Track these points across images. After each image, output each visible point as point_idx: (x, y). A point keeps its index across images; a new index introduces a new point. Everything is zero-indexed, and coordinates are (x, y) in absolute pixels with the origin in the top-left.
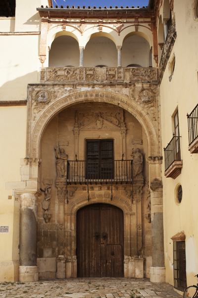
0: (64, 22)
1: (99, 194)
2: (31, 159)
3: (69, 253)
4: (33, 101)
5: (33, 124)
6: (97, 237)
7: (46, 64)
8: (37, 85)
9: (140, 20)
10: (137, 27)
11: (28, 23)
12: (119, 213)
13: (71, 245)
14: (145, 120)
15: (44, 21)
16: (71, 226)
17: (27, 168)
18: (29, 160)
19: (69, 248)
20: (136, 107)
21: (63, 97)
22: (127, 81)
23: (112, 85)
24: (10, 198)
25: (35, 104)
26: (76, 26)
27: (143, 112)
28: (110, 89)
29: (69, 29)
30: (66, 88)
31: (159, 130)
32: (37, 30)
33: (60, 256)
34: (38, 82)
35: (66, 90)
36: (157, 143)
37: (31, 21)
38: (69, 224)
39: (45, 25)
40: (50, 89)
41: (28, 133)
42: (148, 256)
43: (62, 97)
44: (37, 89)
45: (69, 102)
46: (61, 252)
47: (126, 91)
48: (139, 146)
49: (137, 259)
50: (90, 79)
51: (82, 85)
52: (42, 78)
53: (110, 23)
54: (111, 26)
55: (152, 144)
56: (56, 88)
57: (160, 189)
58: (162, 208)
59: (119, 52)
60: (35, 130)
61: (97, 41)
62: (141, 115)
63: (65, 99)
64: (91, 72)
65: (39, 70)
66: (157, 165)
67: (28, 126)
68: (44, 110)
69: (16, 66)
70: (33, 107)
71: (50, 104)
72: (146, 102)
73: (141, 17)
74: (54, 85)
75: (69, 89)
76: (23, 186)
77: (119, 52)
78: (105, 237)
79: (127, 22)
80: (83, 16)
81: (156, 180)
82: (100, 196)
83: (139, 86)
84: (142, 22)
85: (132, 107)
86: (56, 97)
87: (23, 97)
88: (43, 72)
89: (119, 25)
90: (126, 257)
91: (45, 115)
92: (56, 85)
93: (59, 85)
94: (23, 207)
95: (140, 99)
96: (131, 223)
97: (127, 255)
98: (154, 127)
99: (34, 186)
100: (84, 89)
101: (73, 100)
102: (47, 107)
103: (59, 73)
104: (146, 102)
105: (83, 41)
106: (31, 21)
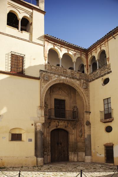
0: (54, 44)
1: (62, 125)
2: (42, 107)
3: (48, 151)
4: (42, 79)
5: (42, 90)
6: (58, 144)
7: (47, 62)
8: (44, 71)
9: (82, 52)
10: (81, 55)
11: (38, 39)
12: (67, 133)
13: (49, 148)
14: (84, 95)
15: (46, 41)
16: (49, 139)
17: (40, 111)
18: (41, 107)
19: (48, 149)
20: (81, 90)
21: (55, 79)
22: (78, 78)
23: (73, 78)
24: (32, 125)
25: (43, 80)
26: (59, 47)
27: (83, 92)
28: (72, 80)
29: (56, 48)
30: (56, 76)
32: (43, 44)
33: (45, 153)
34: (44, 69)
35: (56, 77)
36: (88, 106)
37: (40, 38)
38: (48, 138)
39: (46, 43)
40: (49, 74)
41: (40, 94)
42: (80, 152)
43: (55, 79)
44: (44, 73)
46: (45, 151)
47: (78, 82)
48: (75, 105)
49: (75, 153)
50: (65, 74)
51: (62, 75)
52: (46, 68)
54: (72, 52)
55: (86, 106)
56: (52, 75)
57: (90, 125)
58: (90, 133)
59: (74, 64)
61: (66, 56)
62: (82, 93)
63: (55, 81)
64: (65, 71)
65: (44, 64)
67: (41, 91)
68: (47, 84)
69: (34, 59)
70: (42, 82)
72: (85, 89)
73: (83, 52)
74: (51, 73)
75: (57, 76)
76: (38, 119)
77: (74, 64)
78: (61, 144)
79: (78, 52)
80: (63, 44)
81: (88, 121)
83: (82, 81)
84: (83, 54)
85: (79, 89)
87: (38, 76)
88: (45, 65)
89: (75, 52)
91: (47, 87)
92: (52, 73)
93: (53, 73)
94: (38, 130)
95: (83, 86)
96: (72, 138)
97: (70, 151)
98: (87, 99)
99: (43, 120)
100: (63, 78)
101: (58, 82)
102: (48, 83)
103: (53, 67)
104: (85, 89)
106: (40, 38)
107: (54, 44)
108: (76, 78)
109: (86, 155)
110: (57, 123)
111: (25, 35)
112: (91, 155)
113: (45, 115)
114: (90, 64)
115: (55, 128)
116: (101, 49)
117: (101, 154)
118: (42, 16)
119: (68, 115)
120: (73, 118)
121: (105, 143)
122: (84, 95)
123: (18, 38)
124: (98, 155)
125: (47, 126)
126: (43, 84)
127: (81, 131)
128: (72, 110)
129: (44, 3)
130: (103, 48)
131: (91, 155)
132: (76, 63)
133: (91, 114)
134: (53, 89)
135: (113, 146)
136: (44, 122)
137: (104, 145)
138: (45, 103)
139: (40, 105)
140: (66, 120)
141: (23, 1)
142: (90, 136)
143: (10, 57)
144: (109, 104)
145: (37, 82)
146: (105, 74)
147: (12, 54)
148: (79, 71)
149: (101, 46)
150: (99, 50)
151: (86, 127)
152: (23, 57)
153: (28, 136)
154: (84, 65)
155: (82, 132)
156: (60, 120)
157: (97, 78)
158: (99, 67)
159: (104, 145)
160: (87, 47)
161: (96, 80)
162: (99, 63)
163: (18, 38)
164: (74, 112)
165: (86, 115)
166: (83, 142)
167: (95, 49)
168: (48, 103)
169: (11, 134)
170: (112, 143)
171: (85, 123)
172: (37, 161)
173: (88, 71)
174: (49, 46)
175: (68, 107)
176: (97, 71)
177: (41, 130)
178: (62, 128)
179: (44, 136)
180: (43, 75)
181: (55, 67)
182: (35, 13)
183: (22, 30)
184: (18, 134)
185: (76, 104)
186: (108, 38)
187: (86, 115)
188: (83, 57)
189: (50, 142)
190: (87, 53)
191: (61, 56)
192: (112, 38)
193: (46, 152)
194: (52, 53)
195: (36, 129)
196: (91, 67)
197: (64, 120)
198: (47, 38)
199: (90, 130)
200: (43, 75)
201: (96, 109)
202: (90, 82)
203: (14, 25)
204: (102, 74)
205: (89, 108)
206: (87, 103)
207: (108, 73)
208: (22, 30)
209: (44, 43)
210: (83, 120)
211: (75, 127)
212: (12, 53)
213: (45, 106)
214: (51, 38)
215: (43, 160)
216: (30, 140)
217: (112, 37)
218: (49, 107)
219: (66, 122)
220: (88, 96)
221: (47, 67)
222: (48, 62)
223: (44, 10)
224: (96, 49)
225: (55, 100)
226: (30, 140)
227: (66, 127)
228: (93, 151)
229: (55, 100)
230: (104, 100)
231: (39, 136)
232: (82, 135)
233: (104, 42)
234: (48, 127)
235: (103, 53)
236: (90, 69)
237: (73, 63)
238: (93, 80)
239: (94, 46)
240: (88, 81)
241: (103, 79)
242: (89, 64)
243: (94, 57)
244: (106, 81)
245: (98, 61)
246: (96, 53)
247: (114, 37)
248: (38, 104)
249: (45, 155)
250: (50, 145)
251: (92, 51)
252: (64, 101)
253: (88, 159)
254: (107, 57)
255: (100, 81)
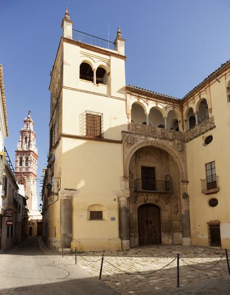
0: (138, 96)
1: (151, 199)
5: (126, 156)
6: (147, 223)
8: (127, 132)
9: (175, 104)
11: (118, 92)
12: (158, 209)
14: (179, 160)
17: (123, 183)
18: (125, 177)
20: (175, 153)
21: (141, 141)
22: (171, 138)
23: (164, 139)
24: (115, 200)
25: (126, 144)
28: (163, 141)
29: (141, 101)
31: (186, 167)
34: (126, 130)
37: (120, 91)
39: (128, 96)
40: (134, 136)
41: (124, 161)
42: (175, 232)
45: (143, 145)
46: (132, 232)
47: (171, 143)
48: (168, 173)
49: (169, 234)
50: (153, 134)
51: (150, 136)
52: (129, 128)
53: (162, 103)
54: (162, 104)
55: (183, 174)
56: (137, 136)
60: (127, 160)
61: (154, 110)
62: (177, 157)
63: (141, 143)
65: (127, 124)
66: (185, 185)
67: (124, 157)
68: (131, 148)
69: (115, 118)
70: (125, 146)
71: (134, 145)
72: (180, 151)
73: (176, 103)
74: (136, 134)
75: (144, 137)
76: (122, 193)
78: (151, 223)
80: (150, 95)
81: (185, 193)
82: (150, 200)
85: (173, 153)
86: (137, 141)
87: (119, 138)
88: (129, 125)
89: (166, 105)
90: (163, 233)
91: (131, 152)
94: (122, 206)
95: (177, 149)
96: (165, 215)
97: (163, 232)
99: (128, 193)
100: (151, 139)
101: (145, 145)
102: (133, 147)
103: (138, 127)
104: (180, 151)
105: (148, 111)
106: (120, 91)
107: (138, 96)
108: (168, 139)
109: (183, 236)
110: (146, 197)
111: (102, 88)
112: (190, 236)
113: (130, 187)
114: (186, 119)
115: (143, 203)
116: (200, 96)
117: (204, 235)
118: (122, 62)
119: (160, 187)
120: (166, 190)
121: (209, 220)
122: (179, 160)
123: (94, 93)
124: (200, 236)
125: (133, 201)
126: (126, 148)
127: (177, 206)
128: (164, 180)
129: (124, 46)
130: (203, 96)
131: (190, 236)
132: (167, 119)
133: (189, 183)
134: (139, 154)
135: (219, 225)
136: (129, 196)
137: (207, 223)
138: (130, 172)
139: (124, 174)
140: (157, 193)
141: (98, 47)
142: (188, 212)
143: (85, 117)
144: (213, 170)
145: (119, 147)
146: (207, 131)
147: (87, 114)
148: (172, 129)
149: (200, 93)
150: (197, 99)
151: (183, 201)
152: (100, 116)
153: (111, 213)
154: (179, 121)
155: (178, 208)
156: (149, 193)
157: (196, 137)
158: (199, 122)
159: (207, 223)
160: (181, 96)
161: (195, 140)
162: (198, 116)
163: (94, 93)
164: (166, 182)
165: (182, 186)
166: (179, 220)
167: (192, 98)
168: (133, 172)
169: (89, 212)
170: (218, 221)
171: (182, 195)
172: (122, 244)
173: (184, 128)
174: (132, 99)
175: (159, 176)
176: (196, 128)
177: (126, 206)
178: (151, 203)
179: (130, 214)
180: (126, 137)
181: (140, 126)
182: (113, 59)
183: (97, 83)
184: (97, 212)
185: (169, 171)
186: (209, 82)
187: (182, 186)
188: (177, 110)
189: (137, 221)
190: (182, 105)
191: (148, 111)
192: (215, 82)
193: (133, 233)
194: (137, 109)
195: (119, 205)
196: (188, 122)
197: (155, 193)
198: (129, 90)
199: (189, 205)
200: (126, 137)
201: (196, 177)
202: (187, 142)
203: (87, 77)
204: (203, 131)
205: (187, 176)
206: (184, 171)
207: (211, 129)
208: (97, 83)
209: (126, 96)
210: (179, 192)
211: (169, 202)
212: (87, 112)
213: (129, 176)
214: (134, 89)
215: (129, 243)
216: (113, 219)
217: (215, 80)
218: (135, 177)
219: (157, 195)
220: (185, 161)
221: (131, 126)
222: (132, 121)
223: (124, 55)
224: (194, 98)
225: (143, 168)
226: (113, 219)
227: (156, 202)
228: (193, 231)
229: (143, 168)
230: (206, 164)
231: (123, 213)
232: (178, 211)
233: (204, 88)
234: (134, 202)
235: (203, 103)
236: (187, 125)
237: (164, 120)
238: (191, 139)
239: (191, 95)
240: (184, 141)
241: (203, 137)
242: (185, 118)
243: (191, 109)
244: (209, 140)
245: (197, 114)
246: (194, 103)
247: (217, 80)
248: (121, 173)
249: (132, 236)
250: (137, 224)
251: (189, 101)
252: (153, 168)
253: (186, 241)
254: (209, 108)
255: (200, 140)
